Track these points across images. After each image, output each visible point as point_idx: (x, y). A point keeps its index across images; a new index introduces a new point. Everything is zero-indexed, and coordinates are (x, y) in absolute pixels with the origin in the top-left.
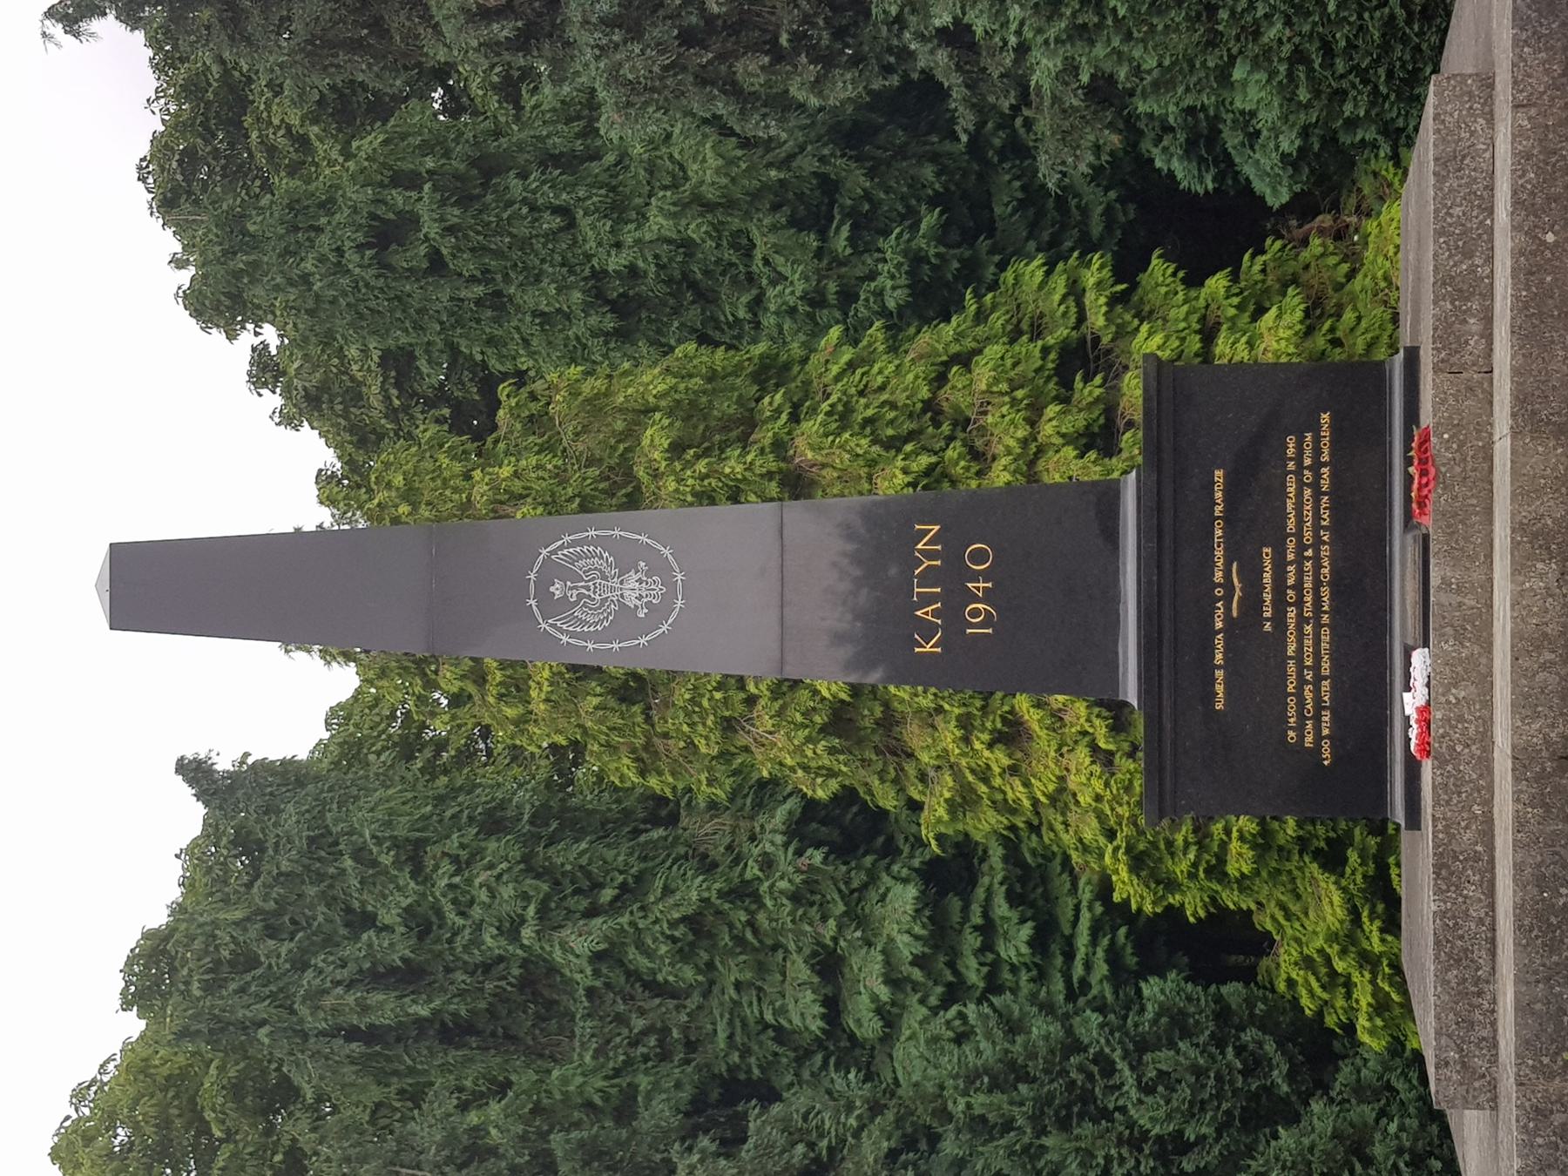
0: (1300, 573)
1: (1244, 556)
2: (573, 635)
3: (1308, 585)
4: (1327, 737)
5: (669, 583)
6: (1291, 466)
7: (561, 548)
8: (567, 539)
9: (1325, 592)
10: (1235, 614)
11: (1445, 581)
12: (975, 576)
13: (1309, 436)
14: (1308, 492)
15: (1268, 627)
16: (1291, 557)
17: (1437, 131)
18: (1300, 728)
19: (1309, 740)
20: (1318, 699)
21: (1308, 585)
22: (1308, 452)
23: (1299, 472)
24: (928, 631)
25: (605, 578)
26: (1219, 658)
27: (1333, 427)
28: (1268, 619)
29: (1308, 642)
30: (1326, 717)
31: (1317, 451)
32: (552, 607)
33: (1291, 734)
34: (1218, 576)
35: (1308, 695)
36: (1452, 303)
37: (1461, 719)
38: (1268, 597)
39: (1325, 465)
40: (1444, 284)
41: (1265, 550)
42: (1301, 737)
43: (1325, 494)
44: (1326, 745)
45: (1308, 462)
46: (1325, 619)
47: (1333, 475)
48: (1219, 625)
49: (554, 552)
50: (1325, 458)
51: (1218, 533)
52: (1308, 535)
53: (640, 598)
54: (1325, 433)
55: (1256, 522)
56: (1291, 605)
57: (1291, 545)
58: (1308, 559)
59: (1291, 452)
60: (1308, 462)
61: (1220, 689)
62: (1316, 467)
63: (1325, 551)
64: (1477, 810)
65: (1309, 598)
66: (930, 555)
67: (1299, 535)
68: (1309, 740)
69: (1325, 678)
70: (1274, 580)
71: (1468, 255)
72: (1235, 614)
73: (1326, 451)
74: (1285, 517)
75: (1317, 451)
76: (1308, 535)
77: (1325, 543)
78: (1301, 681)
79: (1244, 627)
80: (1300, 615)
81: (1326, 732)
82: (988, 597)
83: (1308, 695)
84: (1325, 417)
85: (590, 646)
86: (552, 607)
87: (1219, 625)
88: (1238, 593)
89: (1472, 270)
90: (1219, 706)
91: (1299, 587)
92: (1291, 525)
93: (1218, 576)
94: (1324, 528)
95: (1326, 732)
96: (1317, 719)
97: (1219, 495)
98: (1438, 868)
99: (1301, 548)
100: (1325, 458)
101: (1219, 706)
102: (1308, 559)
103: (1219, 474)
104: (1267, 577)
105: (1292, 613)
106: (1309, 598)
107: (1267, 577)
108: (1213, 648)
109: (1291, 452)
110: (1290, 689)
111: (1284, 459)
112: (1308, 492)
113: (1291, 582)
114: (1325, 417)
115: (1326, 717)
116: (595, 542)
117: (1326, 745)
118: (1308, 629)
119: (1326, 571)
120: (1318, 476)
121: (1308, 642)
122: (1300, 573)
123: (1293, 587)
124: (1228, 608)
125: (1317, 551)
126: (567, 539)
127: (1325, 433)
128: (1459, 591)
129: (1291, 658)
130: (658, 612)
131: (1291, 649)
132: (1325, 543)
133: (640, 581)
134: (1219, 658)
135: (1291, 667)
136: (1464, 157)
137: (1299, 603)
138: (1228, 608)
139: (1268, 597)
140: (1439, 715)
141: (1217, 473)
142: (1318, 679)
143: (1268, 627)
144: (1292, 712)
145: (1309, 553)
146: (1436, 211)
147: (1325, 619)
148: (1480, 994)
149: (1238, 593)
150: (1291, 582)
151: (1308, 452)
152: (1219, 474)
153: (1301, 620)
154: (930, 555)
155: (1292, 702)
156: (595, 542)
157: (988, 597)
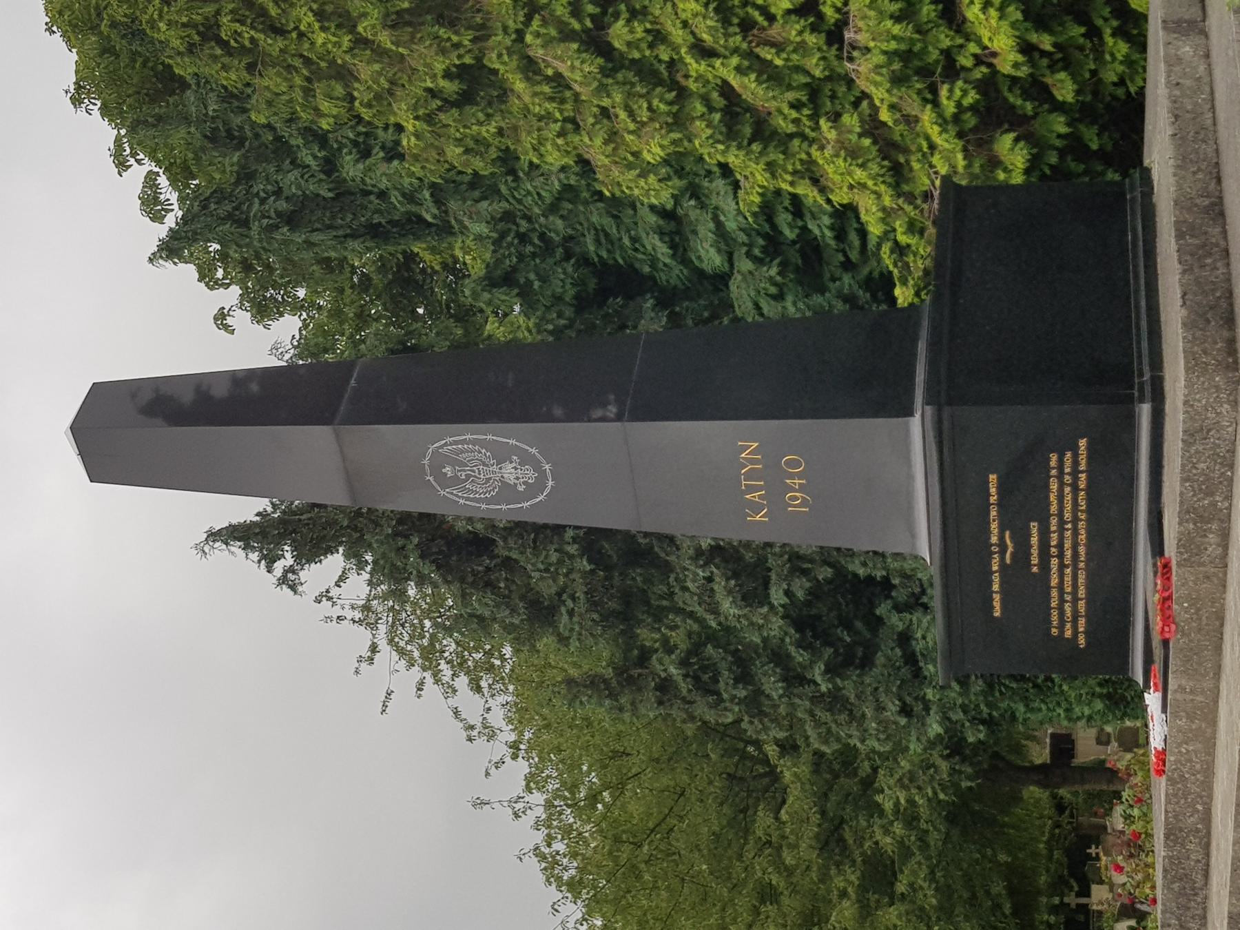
1: (1015, 523)
2: (468, 499)
5: (537, 467)
7: (446, 444)
8: (449, 440)
10: (1008, 561)
11: (1181, 689)
12: (792, 476)
13: (1069, 454)
17: (1186, 412)
18: (1061, 627)
19: (1068, 634)
23: (1060, 476)
24: (757, 508)
25: (484, 464)
26: (996, 587)
27: (1088, 449)
30: (1082, 622)
31: (1076, 463)
32: (444, 481)
33: (1054, 630)
34: (994, 539)
35: (1068, 608)
36: (1195, 524)
37: (1190, 761)
40: (1189, 512)
46: (1082, 565)
47: (1089, 479)
49: (441, 447)
50: (1083, 467)
52: (1067, 515)
53: (517, 478)
55: (1024, 501)
57: (1054, 521)
59: (1053, 463)
62: (1075, 473)
63: (1082, 525)
64: (1200, 807)
66: (752, 462)
67: (1060, 514)
68: (1068, 634)
70: (1040, 541)
71: (1209, 493)
72: (1008, 561)
74: (1049, 504)
75: (1076, 463)
76: (1067, 515)
78: (1062, 601)
79: (1017, 569)
82: (802, 488)
84: (1083, 443)
85: (484, 506)
86: (444, 481)
87: (995, 568)
88: (1010, 550)
89: (1214, 504)
90: (997, 614)
91: (1060, 546)
92: (1054, 508)
93: (994, 539)
95: (1081, 629)
98: (1167, 837)
99: (1062, 522)
100: (1083, 467)
101: (997, 614)
103: (993, 477)
104: (1034, 540)
105: (1054, 562)
107: (1034, 540)
109: (1053, 463)
111: (1048, 469)
112: (1067, 490)
113: (1054, 543)
114: (1083, 443)
116: (474, 442)
118: (1068, 571)
124: (1002, 559)
126: (449, 440)
128: (1192, 692)
130: (534, 489)
131: (1054, 581)
133: (516, 469)
134: (996, 587)
135: (1054, 593)
136: (1209, 430)
137: (1061, 556)
138: (1002, 559)
140: (1172, 759)
141: (991, 477)
143: (1035, 569)
146: (1183, 466)
147: (1082, 565)
148: (1196, 894)
149: (1010, 550)
150: (1054, 543)
152: (993, 477)
153: (1062, 566)
154: (752, 462)
156: (474, 442)
157: (802, 488)
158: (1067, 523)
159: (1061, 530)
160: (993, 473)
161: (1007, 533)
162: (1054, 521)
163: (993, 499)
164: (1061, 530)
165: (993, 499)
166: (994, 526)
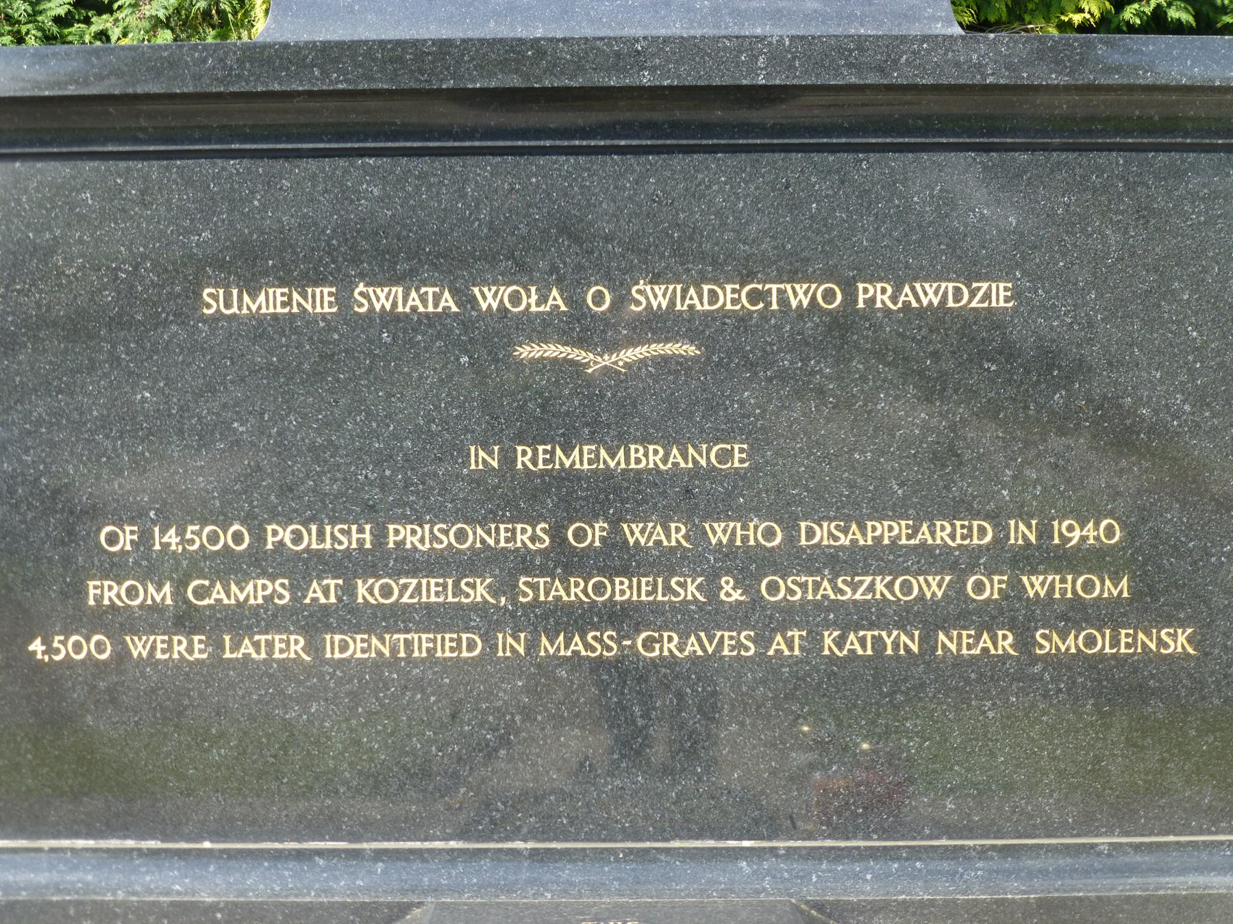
0: (664, 563)
3: (622, 590)
4: (122, 654)
6: (1021, 532)
9: (601, 644)
10: (527, 352)
14: (934, 586)
15: (481, 458)
16: (719, 532)
18: (148, 565)
19: (104, 592)
20: (241, 621)
21: (622, 590)
22: (1068, 586)
26: (382, 298)
28: (508, 458)
29: (432, 590)
30: (190, 649)
33: (127, 537)
34: (652, 296)
35: (255, 591)
38: (581, 458)
39: (1025, 642)
41: (739, 451)
42: (115, 568)
43: (928, 641)
44: (92, 647)
45: (1035, 585)
47: (988, 666)
48: (489, 298)
50: (1047, 643)
51: (800, 295)
52: (790, 589)
54: (1128, 642)
56: (557, 534)
57: (757, 532)
58: (710, 588)
59: (1073, 533)
60: (1035, 585)
61: (271, 301)
62: (1018, 614)
63: (734, 643)
65: (577, 591)
68: (104, 592)
69: (314, 647)
72: (527, 352)
73: (1073, 643)
74: (851, 514)
75: (1075, 614)
76: (790, 589)
77: (763, 641)
80: (524, 562)
81: (138, 647)
83: (255, 591)
84: (1178, 641)
87: (489, 298)
88: (595, 361)
90: (213, 301)
91: (618, 559)
92: (823, 534)
93: (652, 296)
94: (814, 639)
95: (138, 647)
96: (185, 619)
97: (929, 294)
99: (749, 564)
100: (1047, 643)
101: (213, 301)
102: (710, 588)
103: (997, 294)
104: (647, 457)
105: (529, 536)
106: (577, 591)
107: (647, 457)
108: (406, 279)
109: (1073, 533)
110: (279, 534)
112: (934, 586)
113: (635, 533)
114: (1178, 641)
115: (190, 649)
117: (92, 647)
118: (479, 591)
119: (669, 645)
120: (987, 618)
121: (432, 590)
122: (664, 563)
123: (615, 543)
124: (541, 328)
125: (735, 617)
127: (1128, 642)
129: (380, 535)
132: (763, 641)
134: (382, 298)
135: (353, 537)
137: (565, 561)
138: (541, 328)
139: (581, 458)
142: (314, 622)
143: (481, 458)
144: (198, 537)
145: (731, 593)
147: (510, 644)
149: (595, 361)
151: (1068, 586)
152: (997, 294)
155: (232, 537)
158: (746, 581)
159: (713, 563)
160: (1017, 294)
161: (691, 350)
162: (757, 532)
163: (876, 294)
164: (713, 563)
165: (876, 294)
166: (730, 297)
